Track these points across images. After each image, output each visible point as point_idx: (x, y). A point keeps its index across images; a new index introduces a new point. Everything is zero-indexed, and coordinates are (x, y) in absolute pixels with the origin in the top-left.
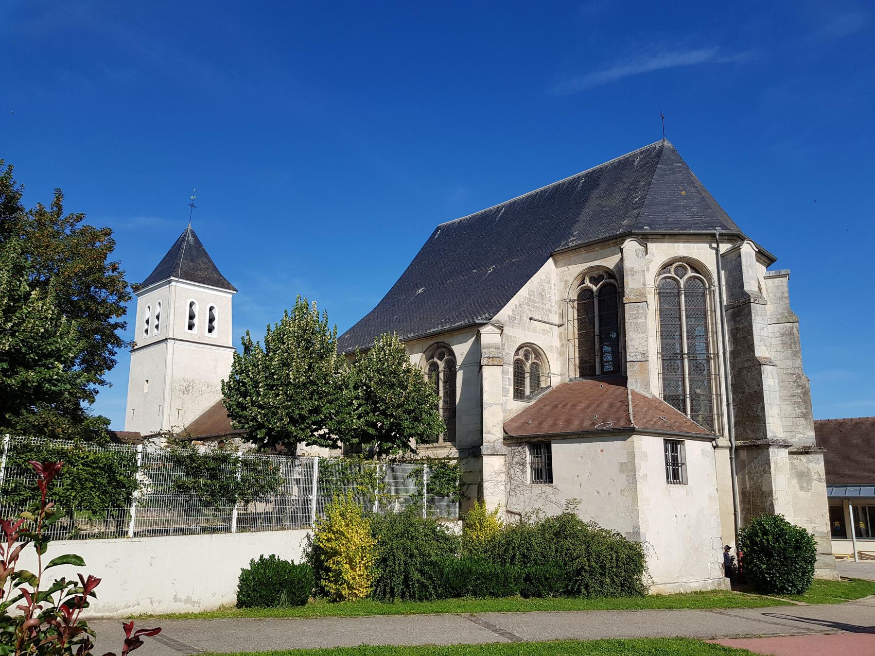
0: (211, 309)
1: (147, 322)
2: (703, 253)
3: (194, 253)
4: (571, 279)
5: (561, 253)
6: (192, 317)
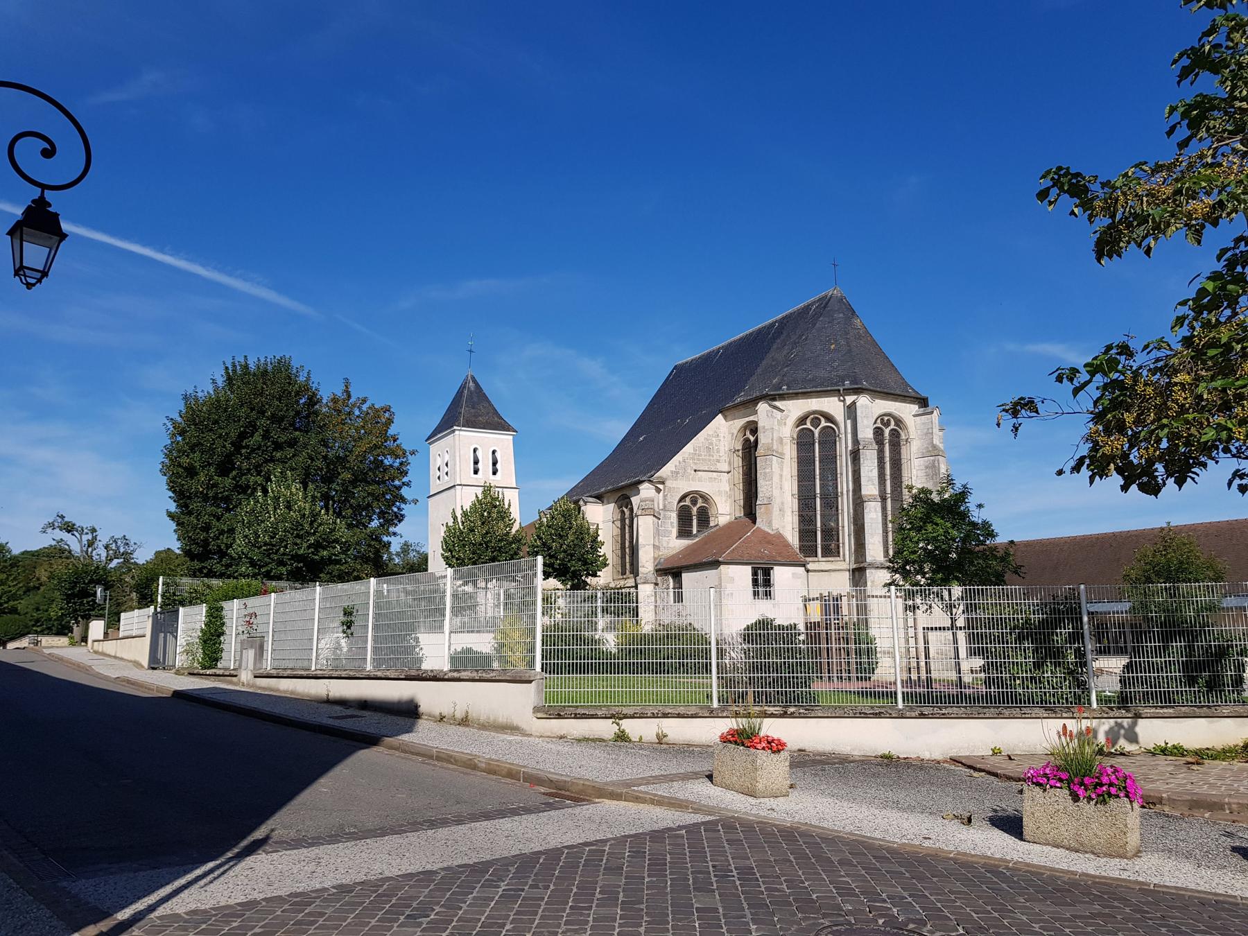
0: (494, 452)
2: (832, 406)
3: (475, 399)
4: (735, 432)
5: (728, 409)
6: (476, 462)
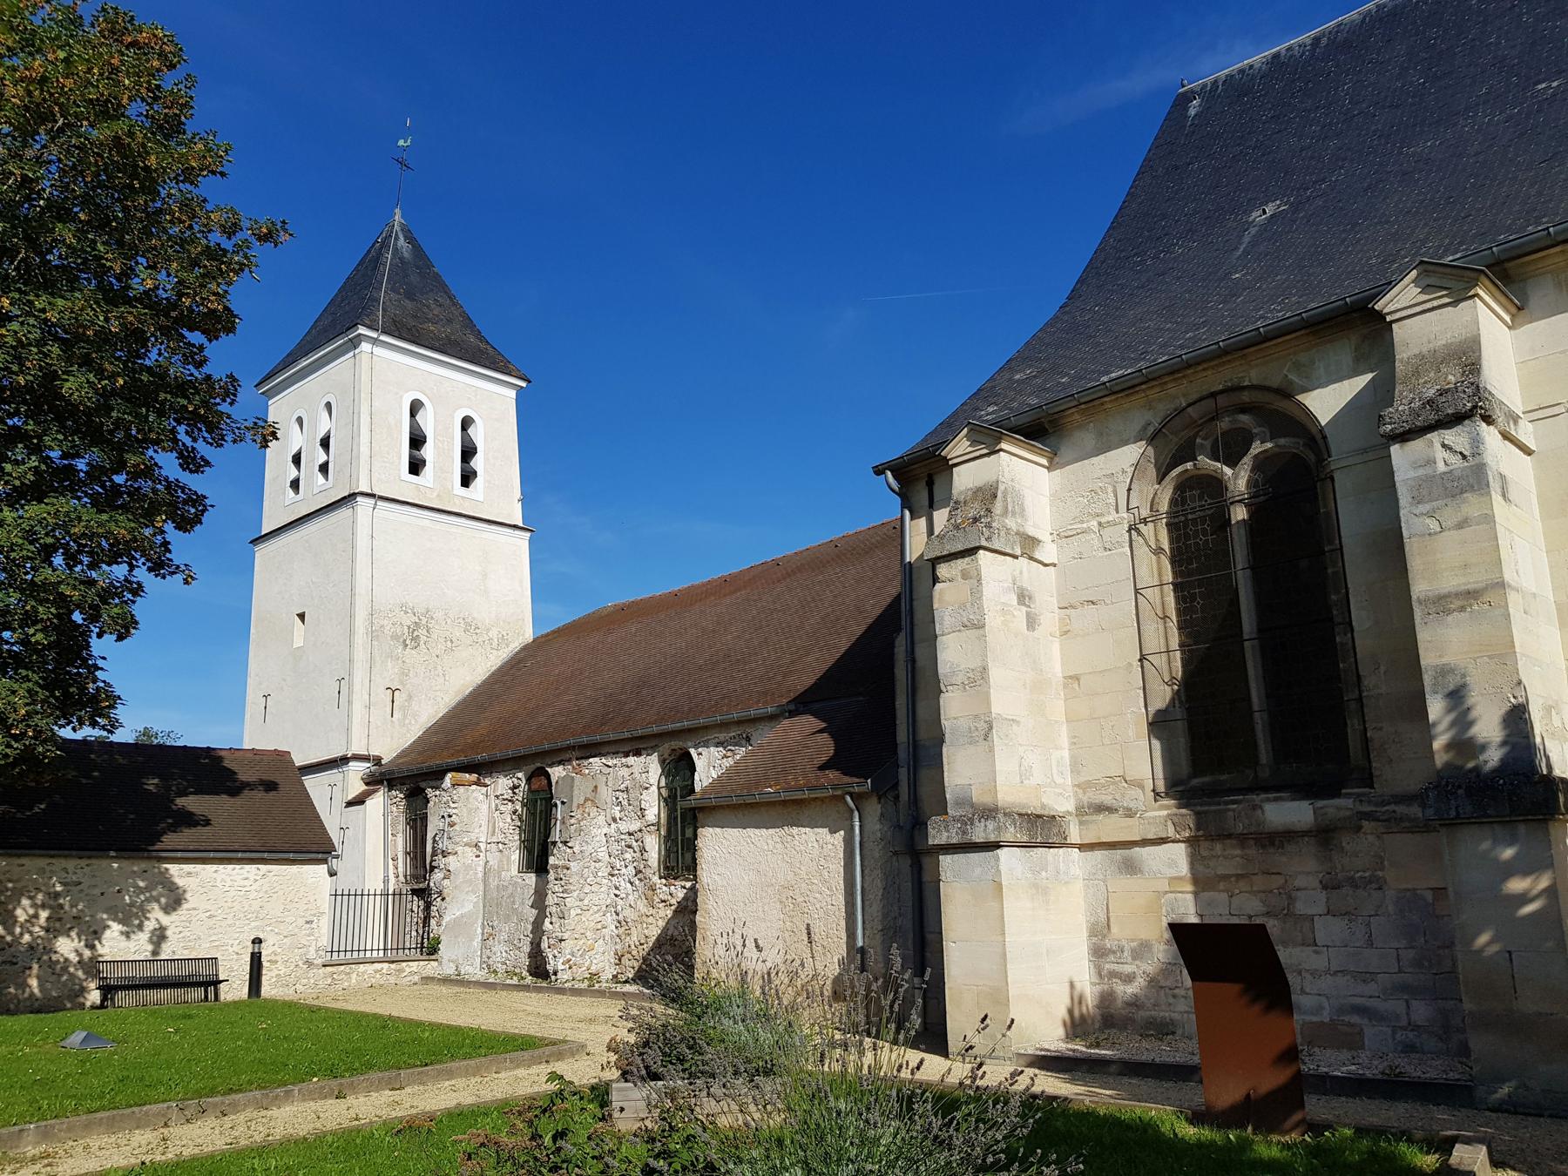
0: (466, 423)
1: (297, 460)
3: (414, 278)
6: (417, 441)
